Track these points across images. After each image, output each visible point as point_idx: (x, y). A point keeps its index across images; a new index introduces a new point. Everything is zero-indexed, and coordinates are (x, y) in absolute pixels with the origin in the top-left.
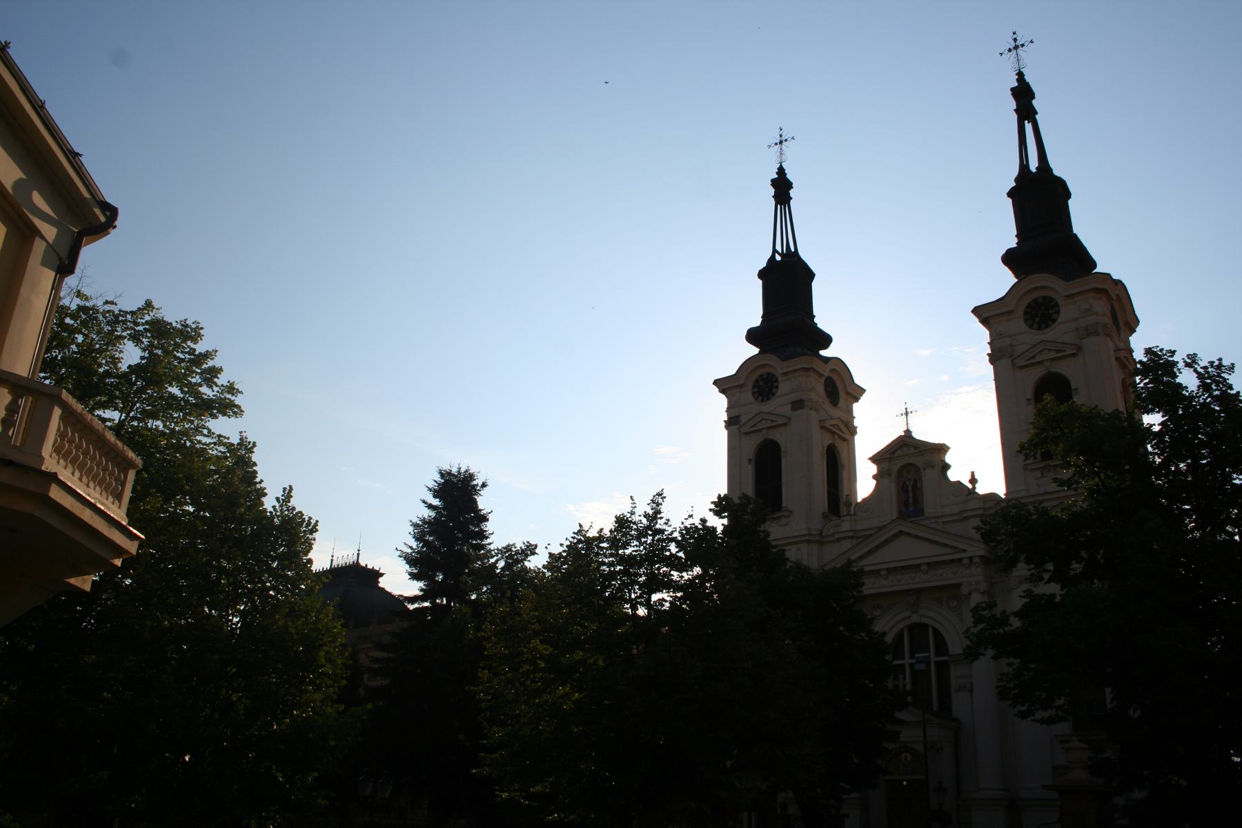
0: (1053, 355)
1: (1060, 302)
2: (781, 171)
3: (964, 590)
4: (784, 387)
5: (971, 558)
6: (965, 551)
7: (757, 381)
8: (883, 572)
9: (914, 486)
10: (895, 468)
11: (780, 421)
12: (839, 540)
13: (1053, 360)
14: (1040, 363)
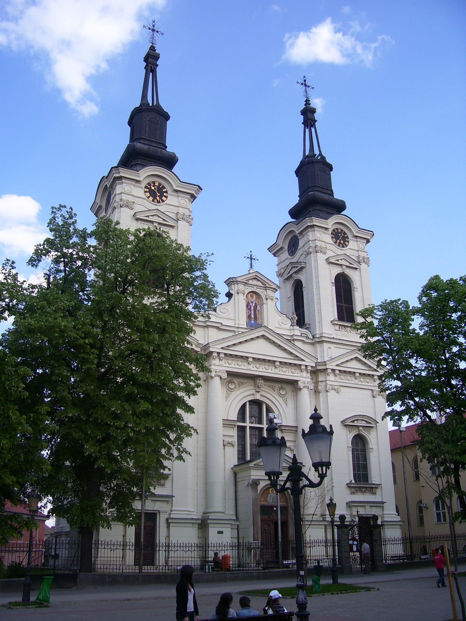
0: (348, 264)
1: (350, 237)
2: (152, 48)
3: (301, 384)
4: (171, 199)
5: (306, 366)
6: (303, 360)
7: (149, 184)
8: (250, 360)
9: (255, 308)
10: (247, 292)
11: (171, 223)
12: (207, 326)
13: (347, 267)
14: (341, 265)
